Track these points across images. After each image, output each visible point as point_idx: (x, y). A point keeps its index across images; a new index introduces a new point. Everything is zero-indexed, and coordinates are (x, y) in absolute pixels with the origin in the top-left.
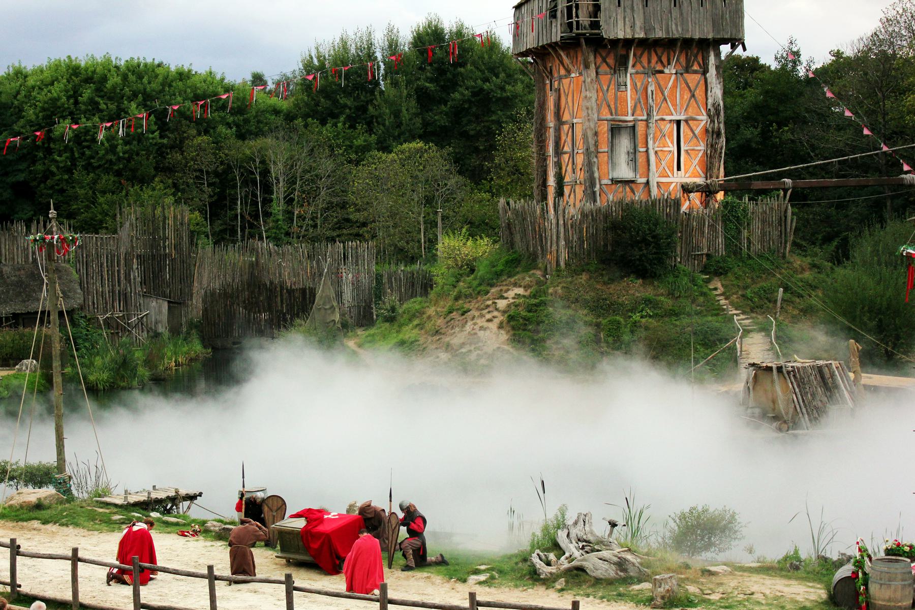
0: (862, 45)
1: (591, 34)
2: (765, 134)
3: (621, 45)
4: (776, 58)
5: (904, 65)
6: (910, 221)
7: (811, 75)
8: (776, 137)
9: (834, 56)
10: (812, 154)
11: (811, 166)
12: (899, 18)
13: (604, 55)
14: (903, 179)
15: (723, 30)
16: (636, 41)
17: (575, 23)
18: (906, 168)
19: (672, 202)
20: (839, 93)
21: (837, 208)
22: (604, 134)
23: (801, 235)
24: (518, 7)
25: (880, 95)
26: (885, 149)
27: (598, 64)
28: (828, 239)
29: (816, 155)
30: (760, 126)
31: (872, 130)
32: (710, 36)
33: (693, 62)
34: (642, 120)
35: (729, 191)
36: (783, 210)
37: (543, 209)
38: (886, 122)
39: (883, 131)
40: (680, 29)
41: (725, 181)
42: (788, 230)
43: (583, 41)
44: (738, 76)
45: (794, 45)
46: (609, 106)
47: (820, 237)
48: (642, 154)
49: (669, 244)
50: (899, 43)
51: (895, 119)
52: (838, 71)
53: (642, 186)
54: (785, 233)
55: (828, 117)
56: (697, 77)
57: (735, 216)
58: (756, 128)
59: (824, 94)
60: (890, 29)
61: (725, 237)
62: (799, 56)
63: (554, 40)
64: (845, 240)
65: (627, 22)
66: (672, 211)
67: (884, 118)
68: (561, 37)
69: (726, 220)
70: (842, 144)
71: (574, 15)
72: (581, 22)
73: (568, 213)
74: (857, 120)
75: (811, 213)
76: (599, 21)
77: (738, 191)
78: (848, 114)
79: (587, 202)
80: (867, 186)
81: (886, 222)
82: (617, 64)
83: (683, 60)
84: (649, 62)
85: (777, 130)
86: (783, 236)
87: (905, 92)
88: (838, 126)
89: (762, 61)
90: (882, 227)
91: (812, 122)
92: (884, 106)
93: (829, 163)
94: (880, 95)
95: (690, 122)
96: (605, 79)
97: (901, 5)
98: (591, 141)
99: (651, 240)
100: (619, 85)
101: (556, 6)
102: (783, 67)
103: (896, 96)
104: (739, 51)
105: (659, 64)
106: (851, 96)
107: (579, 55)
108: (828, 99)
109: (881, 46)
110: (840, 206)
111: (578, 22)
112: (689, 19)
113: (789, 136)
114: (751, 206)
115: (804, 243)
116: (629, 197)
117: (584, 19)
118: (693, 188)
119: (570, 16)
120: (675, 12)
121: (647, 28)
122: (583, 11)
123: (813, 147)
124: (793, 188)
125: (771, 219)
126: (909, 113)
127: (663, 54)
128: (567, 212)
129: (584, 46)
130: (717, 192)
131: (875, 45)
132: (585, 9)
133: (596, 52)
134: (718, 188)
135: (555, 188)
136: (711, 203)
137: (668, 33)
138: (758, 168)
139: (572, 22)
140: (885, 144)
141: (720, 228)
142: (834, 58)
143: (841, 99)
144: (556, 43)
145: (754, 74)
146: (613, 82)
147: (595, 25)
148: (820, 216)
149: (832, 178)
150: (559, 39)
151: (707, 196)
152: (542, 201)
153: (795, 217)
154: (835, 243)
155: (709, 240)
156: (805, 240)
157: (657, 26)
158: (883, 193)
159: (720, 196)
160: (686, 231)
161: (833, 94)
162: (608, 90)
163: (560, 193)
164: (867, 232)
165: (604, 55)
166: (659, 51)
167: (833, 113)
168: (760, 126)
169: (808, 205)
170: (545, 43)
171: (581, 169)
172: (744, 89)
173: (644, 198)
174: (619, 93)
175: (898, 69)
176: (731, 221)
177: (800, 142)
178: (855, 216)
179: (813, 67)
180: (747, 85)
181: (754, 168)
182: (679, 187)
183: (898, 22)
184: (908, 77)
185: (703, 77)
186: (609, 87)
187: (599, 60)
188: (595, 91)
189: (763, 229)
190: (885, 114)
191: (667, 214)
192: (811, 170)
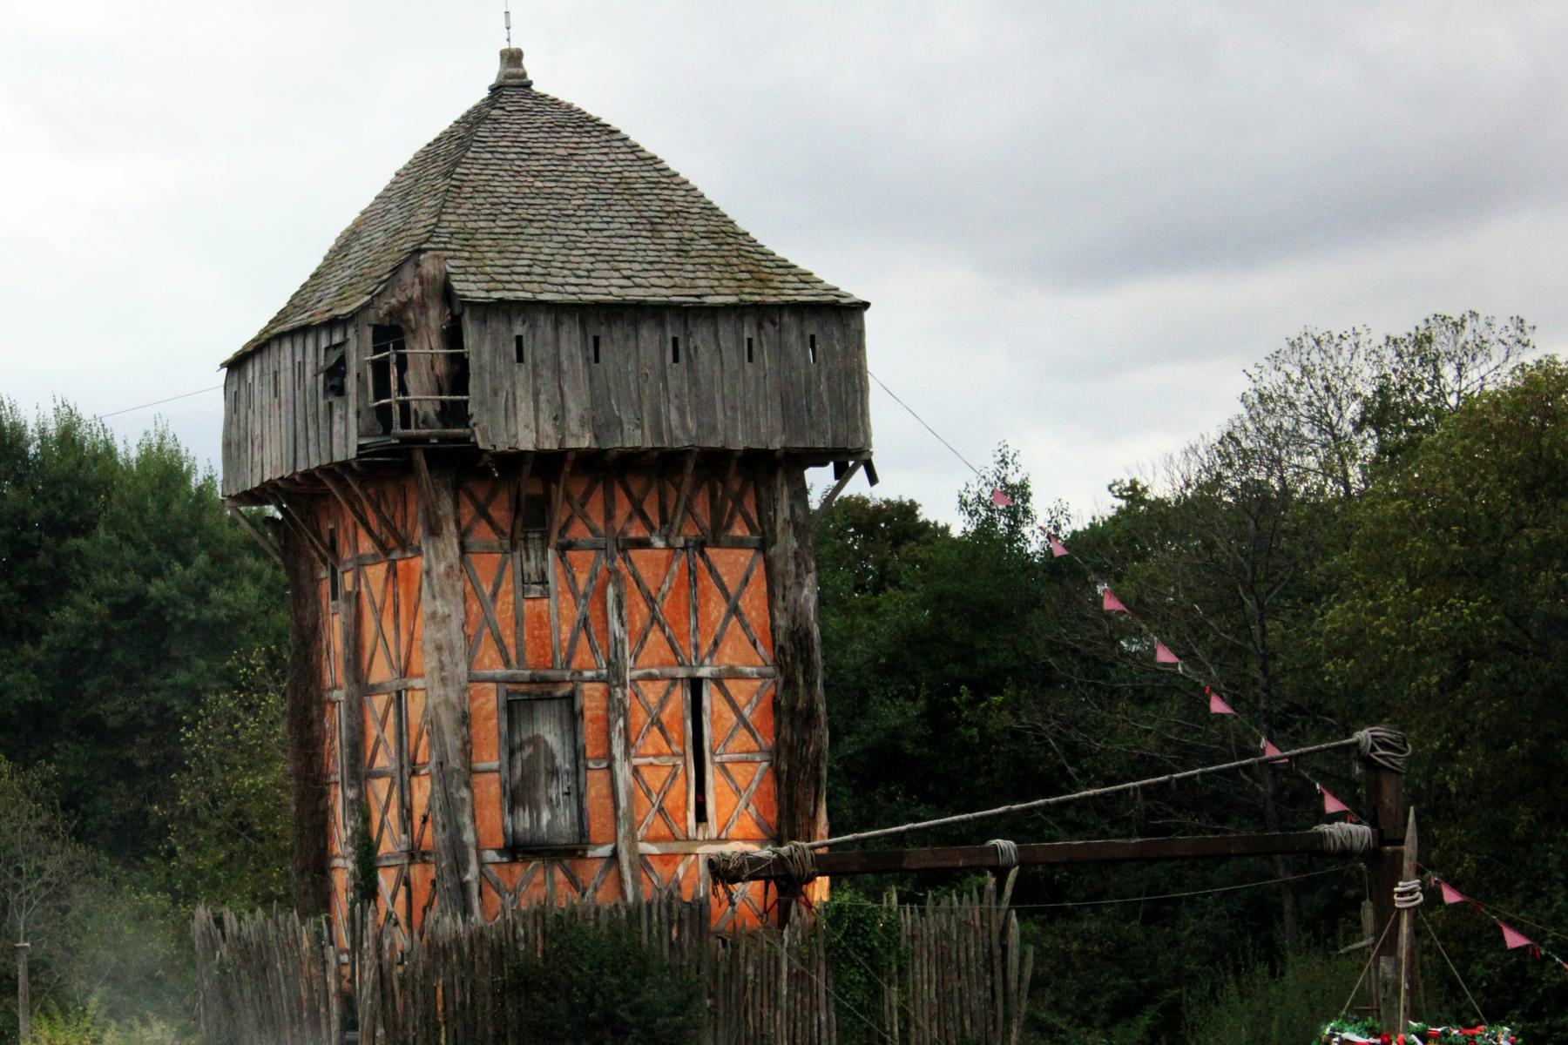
0: (1195, 467)
1: (443, 439)
2: (938, 716)
3: (527, 469)
4: (964, 504)
5: (1310, 519)
6: (1348, 954)
7: (1059, 551)
8: (970, 725)
9: (1121, 497)
10: (1071, 770)
11: (1068, 802)
12: (1291, 393)
13: (481, 496)
14: (1322, 836)
15: (812, 427)
16: (571, 457)
17: (396, 409)
18: (1332, 805)
19: (686, 910)
20: (1140, 601)
21: (1148, 920)
22: (487, 719)
23: (1050, 997)
24: (236, 365)
25: (1250, 604)
26: (1272, 752)
27: (464, 523)
28: (1123, 1010)
29: (1083, 774)
30: (924, 692)
31: (1233, 701)
32: (776, 444)
33: (732, 516)
34: (592, 680)
35: (846, 874)
36: (995, 929)
37: (319, 936)
38: (1272, 679)
39: (1262, 705)
40: (691, 424)
41: (830, 846)
42: (1013, 985)
43: (420, 459)
44: (860, 556)
45: (1011, 468)
46: (499, 641)
47: (1103, 1001)
48: (597, 775)
49: (679, 1029)
50: (1296, 460)
51: (1294, 670)
52: (1134, 540)
53: (598, 867)
54: (1005, 994)
55: (1112, 665)
56: (744, 557)
57: (863, 949)
58: (914, 699)
59: (1098, 601)
60: (1270, 423)
61: (838, 1006)
62: (1026, 497)
63: (338, 457)
64: (1173, 1012)
65: (543, 405)
66: (687, 933)
67: (1264, 668)
68: (360, 447)
69: (837, 959)
70: (1152, 741)
71: (394, 386)
72: (414, 405)
73: (392, 945)
74: (1193, 675)
75: (1076, 937)
76: (466, 402)
77: (870, 877)
78: (1164, 656)
79: (444, 913)
80: (1229, 856)
81: (1282, 958)
82: (519, 522)
83: (702, 507)
84: (609, 516)
85: (971, 705)
86: (1000, 1002)
87: (1319, 595)
88: (1139, 691)
89: (926, 514)
90: (1272, 974)
91: (1069, 682)
92: (1264, 634)
93: (1118, 792)
94: (1250, 604)
95: (730, 684)
96: (485, 565)
97: (1296, 356)
98: (452, 741)
99: (631, 1019)
100: (525, 582)
101: (342, 361)
102: (985, 530)
103: (1296, 607)
104: (857, 485)
105: (637, 522)
106: (1170, 607)
107: (412, 498)
108: (1108, 616)
109: (1246, 468)
110: (1158, 914)
111: (405, 407)
112: (718, 396)
113: (1006, 719)
114: (907, 919)
115: (1060, 1022)
116: (565, 897)
117: (421, 393)
118: (741, 868)
119: (382, 389)
120: (677, 376)
121: (601, 422)
122: (419, 374)
123: (1074, 752)
124: (1022, 863)
125: (962, 955)
126: (1333, 653)
127: (646, 491)
128: (387, 943)
129: (425, 474)
130: (810, 879)
131: (1230, 465)
132: (424, 371)
133: (457, 489)
134: (810, 869)
135: (353, 875)
136: (793, 913)
137: (659, 435)
138: (921, 810)
139: (388, 407)
140: (1271, 740)
141: (820, 981)
142: (1122, 503)
143: (1144, 617)
144: (345, 465)
145: (904, 549)
146: (508, 574)
147: (454, 414)
148: (1100, 944)
149: (1129, 836)
150: (352, 453)
151: (781, 891)
152: (317, 914)
153: (1031, 949)
154: (1145, 1020)
155: (791, 1019)
156: (1062, 1013)
157: (627, 417)
158: (1271, 877)
159: (820, 890)
160: (728, 993)
161: (1123, 602)
162: (494, 595)
163: (366, 889)
164: (1232, 988)
165: (481, 496)
166: (636, 486)
167: (1125, 655)
168: (924, 692)
169: (1068, 915)
170: (315, 464)
171: (425, 820)
172: (878, 588)
173: (604, 898)
174: (527, 604)
175: (1297, 533)
176: (852, 963)
177: (1038, 738)
178: (1195, 942)
179: (1066, 530)
180: (885, 579)
181: (914, 811)
182: (702, 867)
183: (1292, 405)
184: (1326, 556)
185: (760, 559)
186: (497, 586)
187: (468, 511)
188: (460, 600)
189: (941, 983)
190: (1268, 657)
191: (671, 944)
192: (1070, 813)
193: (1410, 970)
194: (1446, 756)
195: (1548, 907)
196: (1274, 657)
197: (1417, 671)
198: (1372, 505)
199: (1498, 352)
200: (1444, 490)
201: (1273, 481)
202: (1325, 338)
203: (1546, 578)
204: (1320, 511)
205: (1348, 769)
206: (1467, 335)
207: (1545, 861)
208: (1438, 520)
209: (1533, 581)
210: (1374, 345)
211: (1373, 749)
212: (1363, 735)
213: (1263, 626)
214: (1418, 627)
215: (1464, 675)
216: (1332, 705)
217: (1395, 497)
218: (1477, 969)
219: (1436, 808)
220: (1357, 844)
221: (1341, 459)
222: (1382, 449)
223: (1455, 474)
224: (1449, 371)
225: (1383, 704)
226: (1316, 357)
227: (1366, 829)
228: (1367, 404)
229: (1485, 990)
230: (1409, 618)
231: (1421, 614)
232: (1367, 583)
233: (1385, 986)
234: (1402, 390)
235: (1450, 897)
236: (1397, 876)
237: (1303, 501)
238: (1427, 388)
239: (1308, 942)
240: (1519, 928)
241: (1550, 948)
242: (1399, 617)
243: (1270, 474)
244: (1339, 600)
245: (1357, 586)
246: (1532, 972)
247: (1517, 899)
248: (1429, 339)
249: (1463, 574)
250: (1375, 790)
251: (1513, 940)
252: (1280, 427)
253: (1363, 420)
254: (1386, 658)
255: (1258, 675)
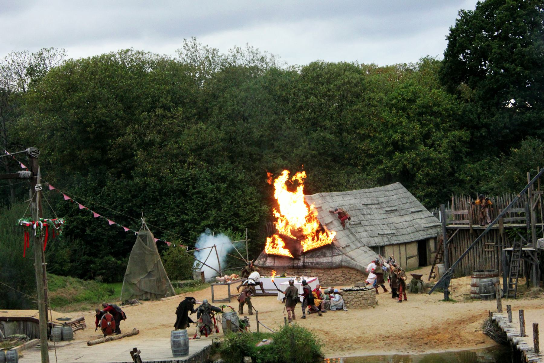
5: (16, 98)
6: (27, 202)
12: (10, 66)
14: (19, 174)
18: (23, 166)
39: (5, 143)
50: (11, 83)
51: (12, 134)
60: (5, 74)
67: (5, 134)
81: (11, 204)
90: (8, 208)
92: (5, 125)
126: (22, 130)
158: (8, 184)
175: (12, 100)
183: (10, 69)
184: (19, 106)
193: (39, 205)
194: (49, 154)
195: (74, 190)
196: (7, 131)
197: (42, 134)
198: (30, 94)
199: (59, 57)
200: (47, 90)
201: (6, 88)
202: (17, 53)
203: (72, 111)
204: (17, 95)
205: (25, 158)
206: (51, 53)
207: (73, 179)
208: (46, 97)
209: (69, 112)
210: (29, 55)
211: (31, 153)
212: (29, 150)
213: (4, 123)
214: (42, 123)
215: (53, 135)
216: (22, 142)
217: (36, 92)
218: (58, 205)
219: (46, 167)
220: (27, 176)
221: (23, 83)
222: (32, 81)
223: (50, 86)
224: (47, 62)
225: (34, 142)
226: (16, 58)
227: (30, 172)
228: (28, 70)
229: (60, 210)
230: (39, 121)
231: (43, 120)
232: (30, 113)
233: (33, 210)
234: (36, 66)
235: (51, 188)
236: (36, 183)
237: (13, 93)
238: (42, 65)
239: (17, 200)
240: (68, 195)
241: (74, 200)
242: (37, 121)
243: (5, 86)
244: (23, 117)
245: (27, 113)
246: (70, 206)
247: (67, 188)
248: (42, 54)
249: (53, 111)
250: (32, 162)
251: (66, 198)
252: (7, 75)
253: (27, 73)
254: (34, 131)
255: (3, 135)
